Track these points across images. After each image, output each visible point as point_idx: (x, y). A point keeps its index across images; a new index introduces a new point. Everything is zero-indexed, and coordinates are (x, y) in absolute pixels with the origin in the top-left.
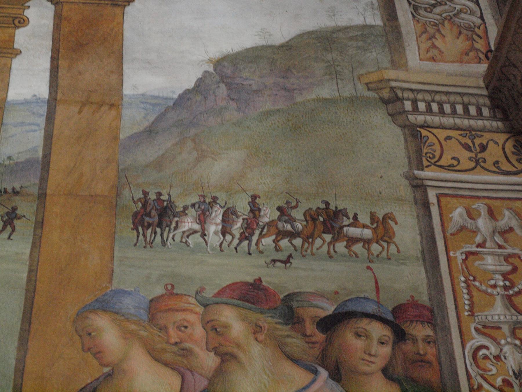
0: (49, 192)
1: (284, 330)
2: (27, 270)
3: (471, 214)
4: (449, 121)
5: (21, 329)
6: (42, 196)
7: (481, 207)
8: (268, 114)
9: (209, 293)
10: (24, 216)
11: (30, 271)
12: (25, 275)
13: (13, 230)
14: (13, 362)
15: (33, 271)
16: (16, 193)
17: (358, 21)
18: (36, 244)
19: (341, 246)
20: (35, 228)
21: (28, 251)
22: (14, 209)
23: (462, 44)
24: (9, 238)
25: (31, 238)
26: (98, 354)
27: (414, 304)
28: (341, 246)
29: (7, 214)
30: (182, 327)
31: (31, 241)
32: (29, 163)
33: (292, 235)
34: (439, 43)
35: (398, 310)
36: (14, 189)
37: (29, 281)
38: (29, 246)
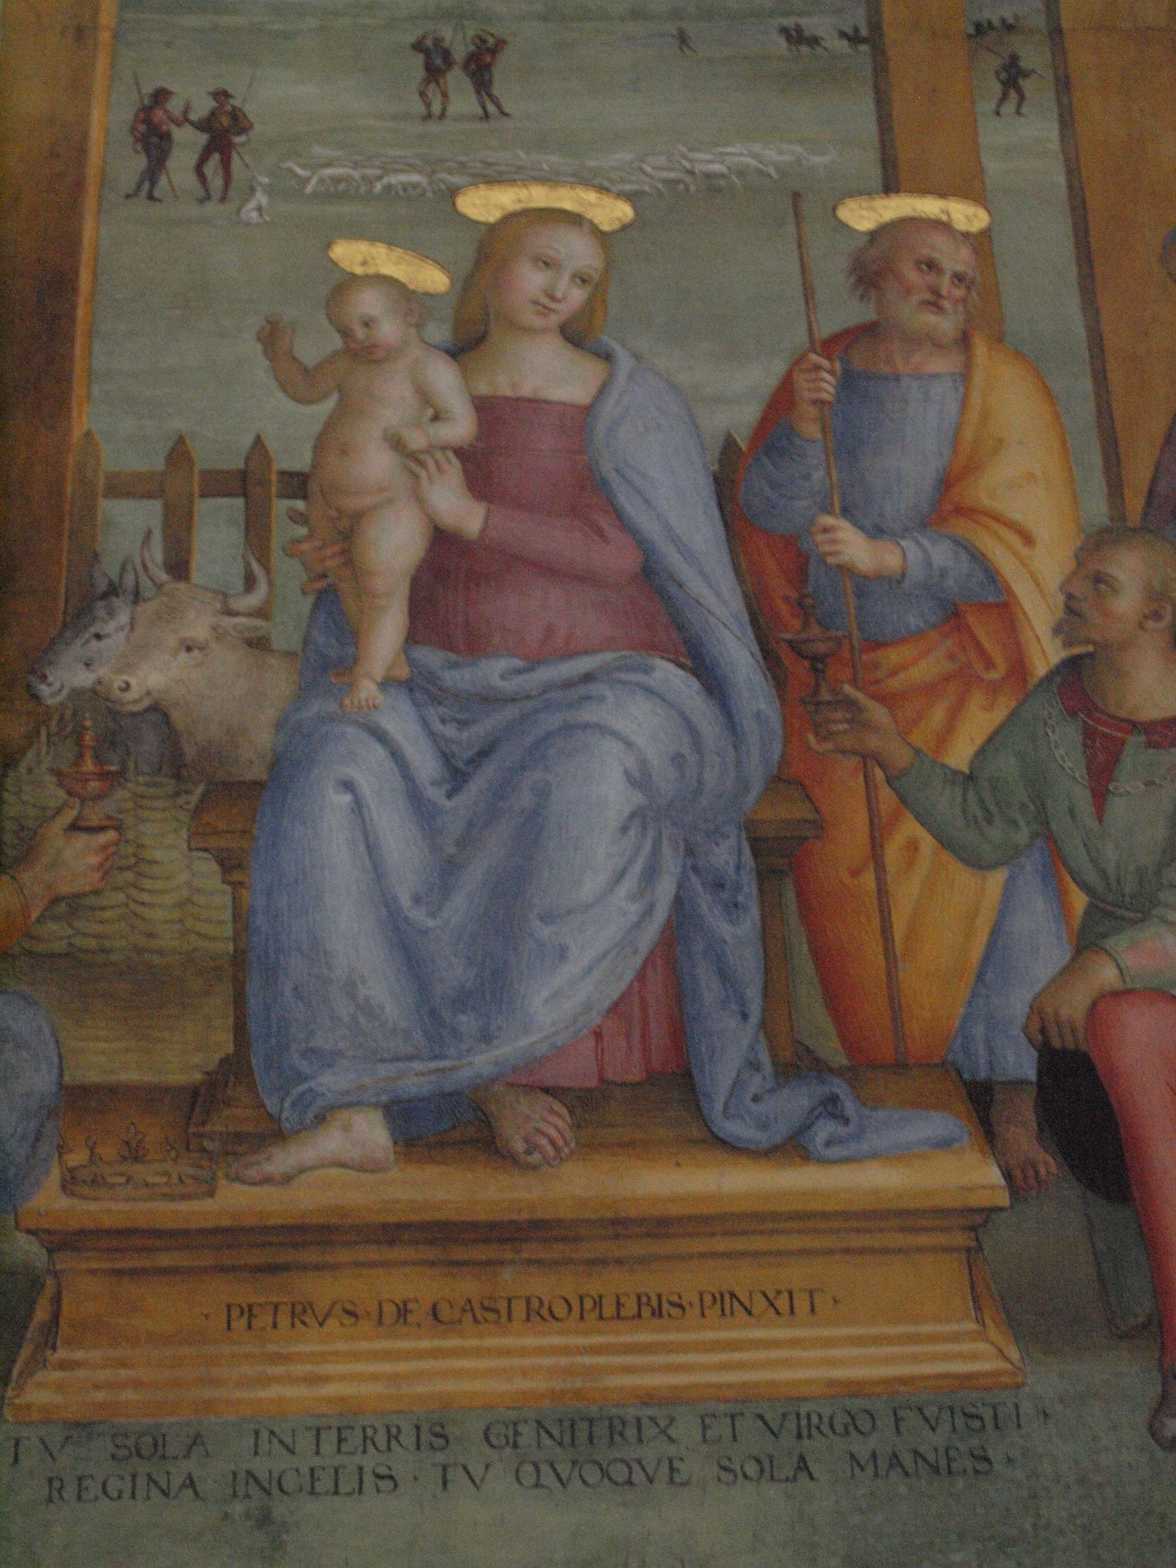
0: (1065, 25)
2: (1061, 169)
5: (1079, 273)
6: (1056, 33)
10: (1033, 71)
11: (1069, 172)
12: (1061, 179)
13: (1022, 97)
14: (1082, 333)
15: (1072, 171)
16: (1009, 28)
18: (1067, 122)
20: (1058, 93)
21: (1055, 134)
22: (1014, 59)
24: (1018, 113)
25: (1055, 110)
29: (1006, 68)
31: (1055, 116)
36: (1003, 20)
37: (1070, 187)
38: (1056, 126)
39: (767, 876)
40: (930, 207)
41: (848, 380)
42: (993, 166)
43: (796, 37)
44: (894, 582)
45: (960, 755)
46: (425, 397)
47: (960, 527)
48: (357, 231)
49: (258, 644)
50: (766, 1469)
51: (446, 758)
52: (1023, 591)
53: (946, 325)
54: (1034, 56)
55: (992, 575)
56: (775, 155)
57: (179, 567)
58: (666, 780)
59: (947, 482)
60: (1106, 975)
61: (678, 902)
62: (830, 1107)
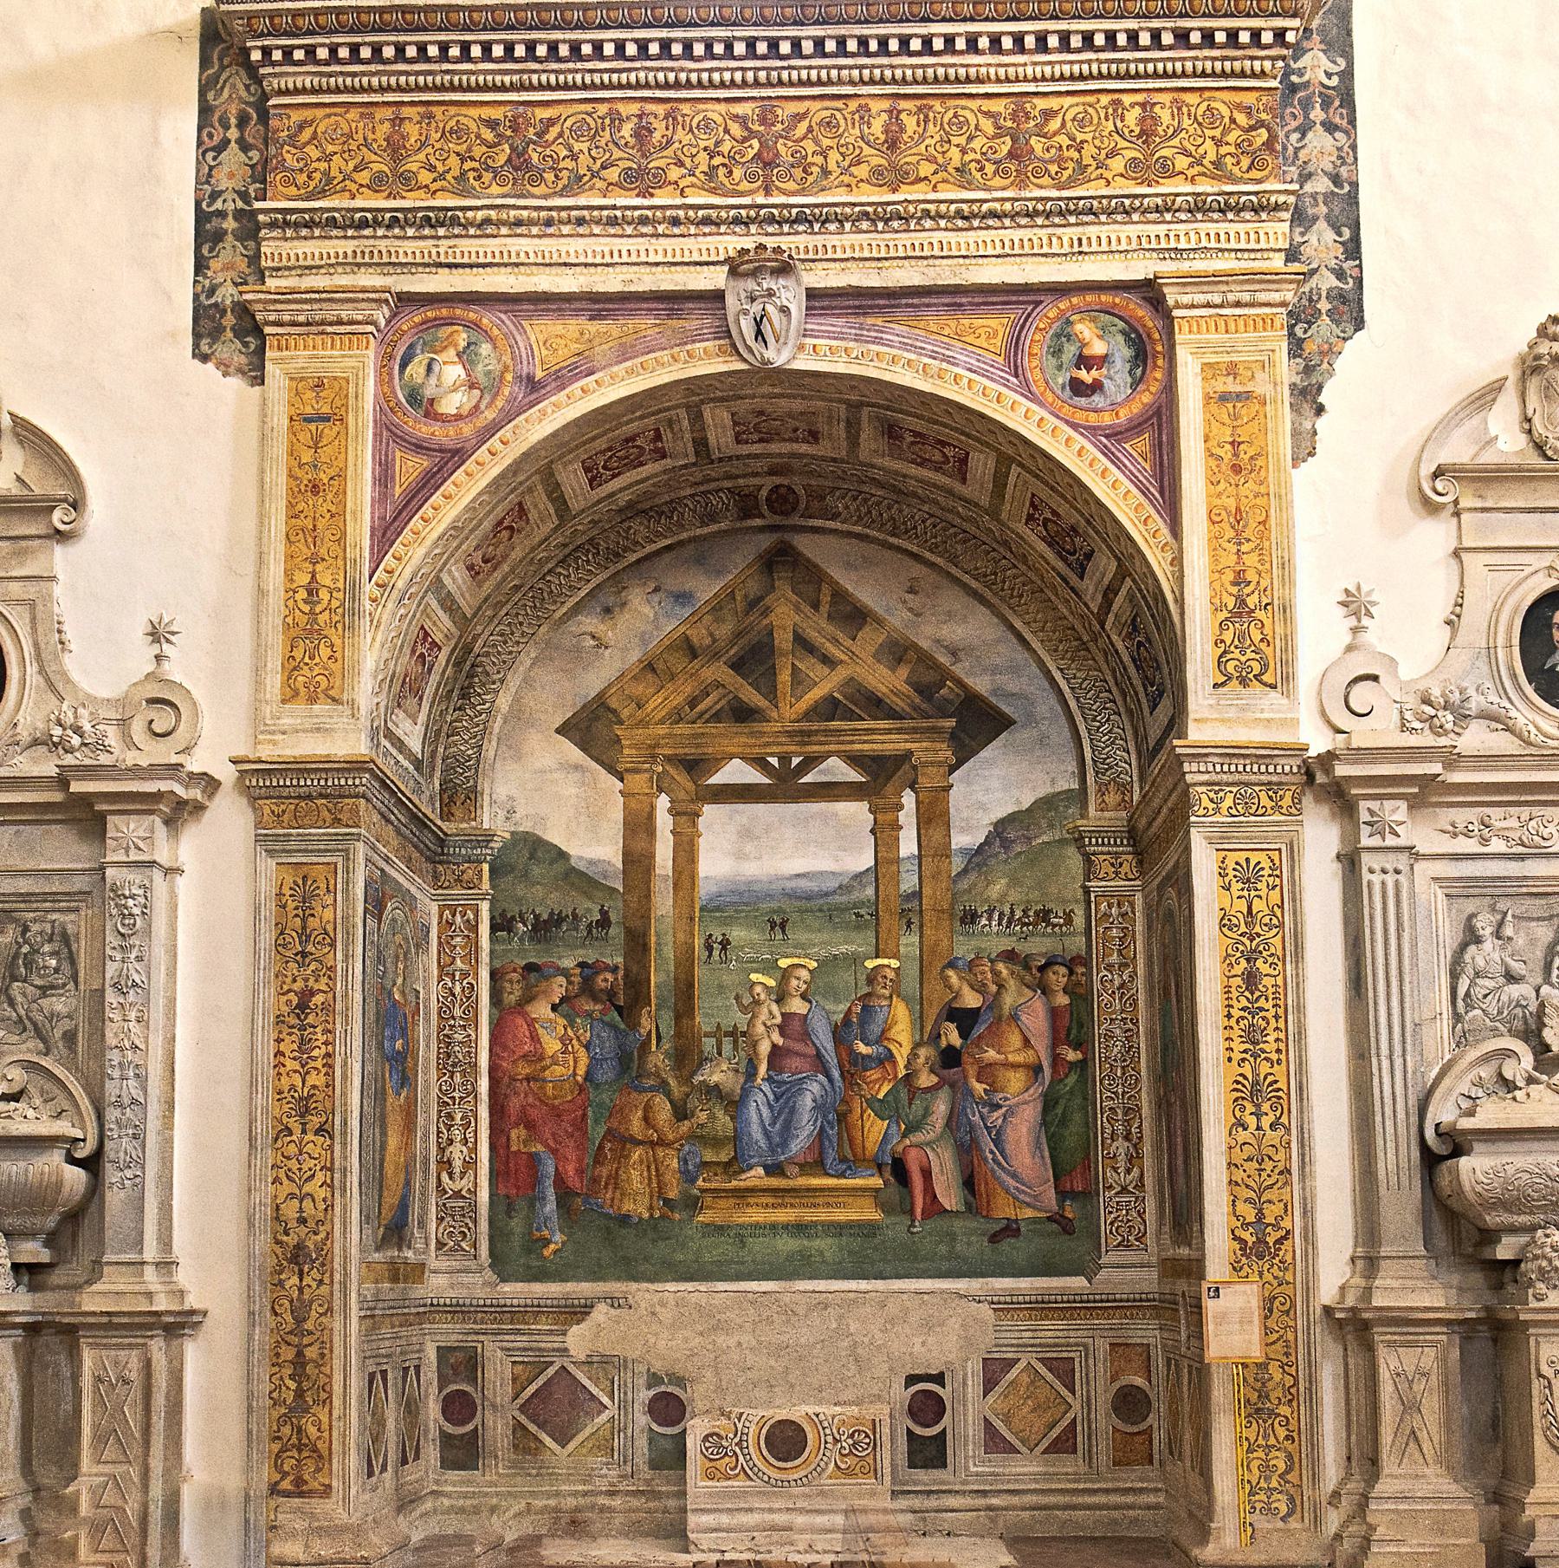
1: (1023, 973)
3: (1110, 906)
4: (1105, 849)
7: (1115, 901)
8: (1020, 853)
9: (993, 956)
17: (1066, 787)
18: (921, 937)
19: (1049, 930)
23: (1118, 798)
26: (950, 988)
27: (1079, 956)
28: (1049, 930)
30: (983, 973)
32: (914, 893)
33: (1027, 925)
34: (1106, 798)
35: (1072, 959)
39: (839, 1121)
40: (885, 961)
41: (864, 1008)
42: (902, 949)
43: (858, 915)
44: (869, 1056)
45: (881, 1096)
46: (770, 1013)
47: (886, 1043)
48: (757, 971)
49: (737, 1071)
50: (834, 1236)
51: (774, 1093)
52: (899, 1058)
53: (886, 992)
54: (915, 920)
55: (892, 1055)
56: (851, 948)
57: (720, 1054)
58: (820, 1101)
59: (883, 1032)
60: (908, 1142)
61: (822, 1127)
62: (850, 1168)
